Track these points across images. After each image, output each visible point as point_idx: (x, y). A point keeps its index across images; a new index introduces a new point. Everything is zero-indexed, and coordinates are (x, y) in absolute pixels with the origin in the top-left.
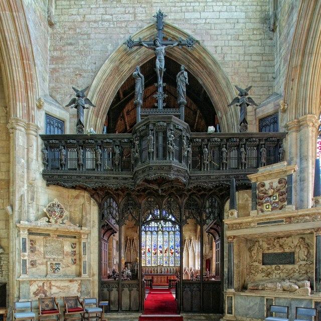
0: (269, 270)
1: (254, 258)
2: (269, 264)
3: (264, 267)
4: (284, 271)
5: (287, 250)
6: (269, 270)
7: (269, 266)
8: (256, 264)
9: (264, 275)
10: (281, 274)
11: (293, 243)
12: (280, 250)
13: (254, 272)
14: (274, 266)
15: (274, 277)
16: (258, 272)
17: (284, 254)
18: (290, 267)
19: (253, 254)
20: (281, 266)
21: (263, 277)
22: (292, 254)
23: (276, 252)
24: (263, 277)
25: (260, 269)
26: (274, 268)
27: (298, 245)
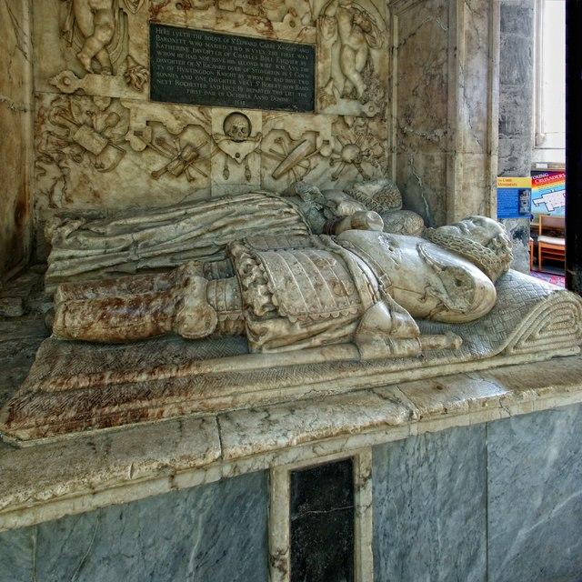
0: (190, 136)
1: (96, 44)
2: (192, 100)
3: (159, 111)
5: (283, 32)
6: (190, 136)
7: (192, 113)
8: (111, 87)
9: (159, 163)
10: (255, 164)
12: (253, 20)
13: (95, 144)
14: (218, 114)
15: (217, 176)
16: (122, 147)
17: (265, 47)
18: (297, 123)
19: (86, 17)
20: (256, 116)
21: (155, 175)
22: (306, 55)
23: (227, 27)
24: (155, 175)
25: (138, 123)
26: (217, 127)
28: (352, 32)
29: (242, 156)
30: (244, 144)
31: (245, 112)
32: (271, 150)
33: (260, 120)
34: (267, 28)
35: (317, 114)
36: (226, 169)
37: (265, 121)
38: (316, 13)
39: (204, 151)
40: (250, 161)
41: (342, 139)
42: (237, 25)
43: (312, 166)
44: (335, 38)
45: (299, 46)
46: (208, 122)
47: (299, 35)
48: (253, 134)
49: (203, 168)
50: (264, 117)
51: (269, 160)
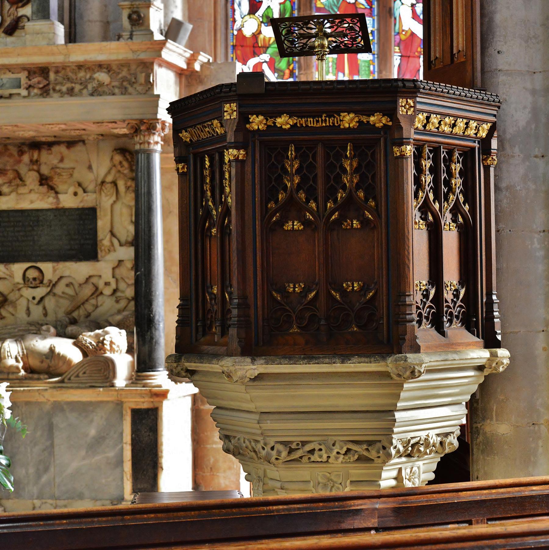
4: (60, 289)
11: (90, 168)
23: (25, 205)
26: (18, 278)
27: (110, 179)
28: (126, 192)
29: (38, 299)
30: (38, 289)
31: (39, 265)
32: (63, 293)
33: (51, 270)
34: (55, 200)
35: (98, 261)
36: (28, 309)
37: (55, 270)
38: (99, 181)
39: (11, 297)
40: (47, 301)
41: (127, 280)
42: (32, 202)
43: (99, 304)
44: (114, 198)
45: (83, 209)
46: (12, 276)
47: (81, 202)
48: (45, 281)
49: (11, 309)
50: (54, 267)
51: (62, 301)
